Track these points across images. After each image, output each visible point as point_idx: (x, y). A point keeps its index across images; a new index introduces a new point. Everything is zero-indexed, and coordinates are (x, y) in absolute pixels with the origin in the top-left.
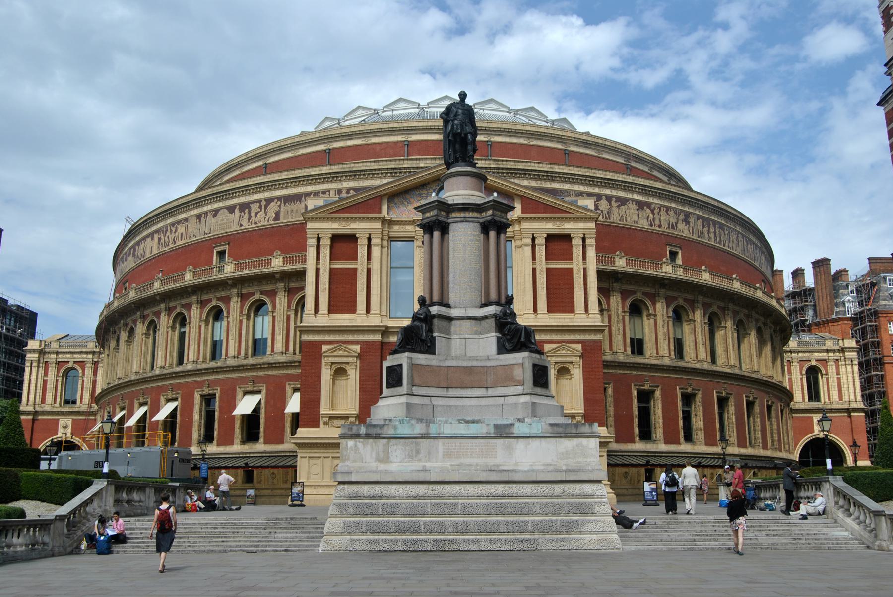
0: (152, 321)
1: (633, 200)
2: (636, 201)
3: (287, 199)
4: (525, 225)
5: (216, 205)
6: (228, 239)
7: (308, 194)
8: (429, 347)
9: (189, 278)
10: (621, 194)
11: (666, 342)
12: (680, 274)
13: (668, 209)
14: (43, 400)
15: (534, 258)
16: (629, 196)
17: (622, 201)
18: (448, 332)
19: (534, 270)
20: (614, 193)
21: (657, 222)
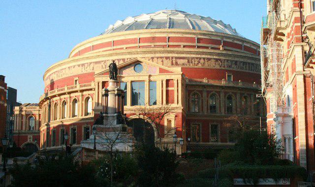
0: (56, 103)
1: (213, 58)
2: (215, 59)
3: (96, 63)
4: (160, 76)
5: (74, 64)
6: (79, 76)
7: (103, 61)
8: (102, 123)
9: (66, 90)
10: (209, 57)
11: (224, 108)
12: (231, 85)
13: (228, 60)
14: (22, 129)
15: (162, 87)
16: (212, 57)
17: (209, 59)
18: (107, 119)
19: (162, 90)
20: (206, 56)
21: (223, 65)
